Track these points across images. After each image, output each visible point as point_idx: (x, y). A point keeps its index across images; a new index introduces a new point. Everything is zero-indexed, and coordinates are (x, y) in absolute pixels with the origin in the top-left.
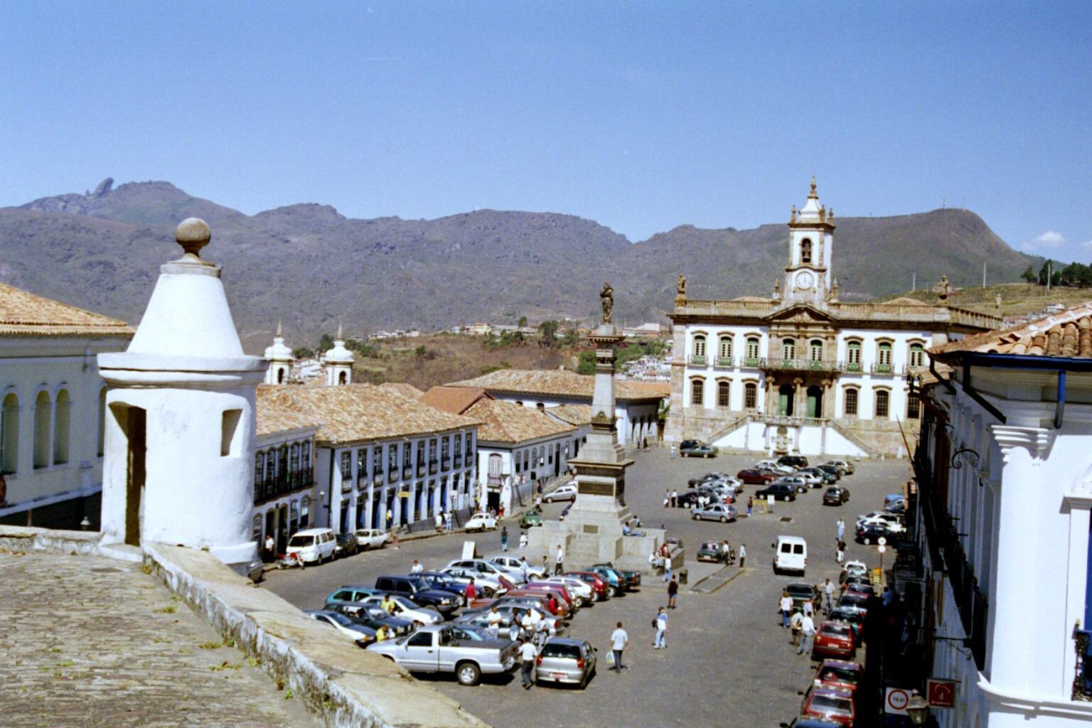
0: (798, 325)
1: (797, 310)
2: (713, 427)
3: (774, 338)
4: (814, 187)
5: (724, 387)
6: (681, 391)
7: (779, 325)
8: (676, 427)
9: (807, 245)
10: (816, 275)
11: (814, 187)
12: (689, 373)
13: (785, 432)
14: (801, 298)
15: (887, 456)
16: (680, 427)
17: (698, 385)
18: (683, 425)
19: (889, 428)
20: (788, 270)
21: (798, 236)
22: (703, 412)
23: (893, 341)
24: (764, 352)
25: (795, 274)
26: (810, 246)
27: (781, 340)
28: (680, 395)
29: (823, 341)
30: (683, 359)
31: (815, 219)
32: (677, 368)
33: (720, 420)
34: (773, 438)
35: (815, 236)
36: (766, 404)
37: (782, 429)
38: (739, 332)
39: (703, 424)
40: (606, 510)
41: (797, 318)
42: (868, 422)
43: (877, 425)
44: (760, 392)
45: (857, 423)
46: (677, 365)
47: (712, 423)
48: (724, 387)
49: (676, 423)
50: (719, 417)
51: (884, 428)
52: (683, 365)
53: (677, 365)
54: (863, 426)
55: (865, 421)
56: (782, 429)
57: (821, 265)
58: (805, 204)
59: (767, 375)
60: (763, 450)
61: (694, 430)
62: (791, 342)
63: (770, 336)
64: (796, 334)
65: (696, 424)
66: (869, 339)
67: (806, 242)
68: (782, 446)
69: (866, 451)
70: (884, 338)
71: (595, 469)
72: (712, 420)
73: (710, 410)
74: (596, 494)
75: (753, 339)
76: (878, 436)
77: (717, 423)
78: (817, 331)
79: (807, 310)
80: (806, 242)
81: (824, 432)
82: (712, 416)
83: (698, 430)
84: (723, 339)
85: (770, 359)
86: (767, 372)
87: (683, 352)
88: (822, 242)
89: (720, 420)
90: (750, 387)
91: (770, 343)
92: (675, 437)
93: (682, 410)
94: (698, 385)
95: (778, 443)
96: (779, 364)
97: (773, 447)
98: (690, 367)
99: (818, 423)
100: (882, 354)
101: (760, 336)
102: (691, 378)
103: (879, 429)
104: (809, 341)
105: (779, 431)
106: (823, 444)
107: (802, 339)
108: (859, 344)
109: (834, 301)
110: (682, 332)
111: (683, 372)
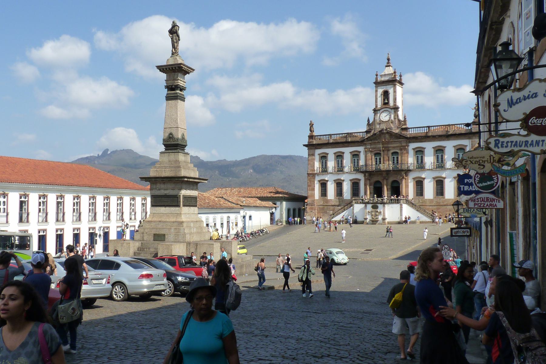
4: (388, 59)
5: (339, 184)
6: (313, 189)
11: (388, 59)
13: (377, 207)
14: (384, 126)
17: (324, 185)
19: (445, 203)
22: (327, 201)
23: (445, 147)
24: (362, 162)
29: (399, 151)
30: (314, 170)
37: (375, 207)
38: (347, 151)
43: (437, 202)
51: (442, 204)
54: (428, 204)
56: (375, 207)
59: (365, 176)
60: (363, 220)
61: (322, 213)
62: (379, 154)
65: (323, 209)
67: (386, 94)
78: (394, 146)
80: (386, 94)
81: (401, 208)
82: (333, 204)
83: (324, 212)
84: (337, 156)
86: (364, 172)
90: (355, 185)
93: (314, 201)
95: (372, 215)
99: (397, 201)
100: (438, 157)
105: (373, 207)
106: (401, 215)
109: (404, 127)
110: (313, 155)
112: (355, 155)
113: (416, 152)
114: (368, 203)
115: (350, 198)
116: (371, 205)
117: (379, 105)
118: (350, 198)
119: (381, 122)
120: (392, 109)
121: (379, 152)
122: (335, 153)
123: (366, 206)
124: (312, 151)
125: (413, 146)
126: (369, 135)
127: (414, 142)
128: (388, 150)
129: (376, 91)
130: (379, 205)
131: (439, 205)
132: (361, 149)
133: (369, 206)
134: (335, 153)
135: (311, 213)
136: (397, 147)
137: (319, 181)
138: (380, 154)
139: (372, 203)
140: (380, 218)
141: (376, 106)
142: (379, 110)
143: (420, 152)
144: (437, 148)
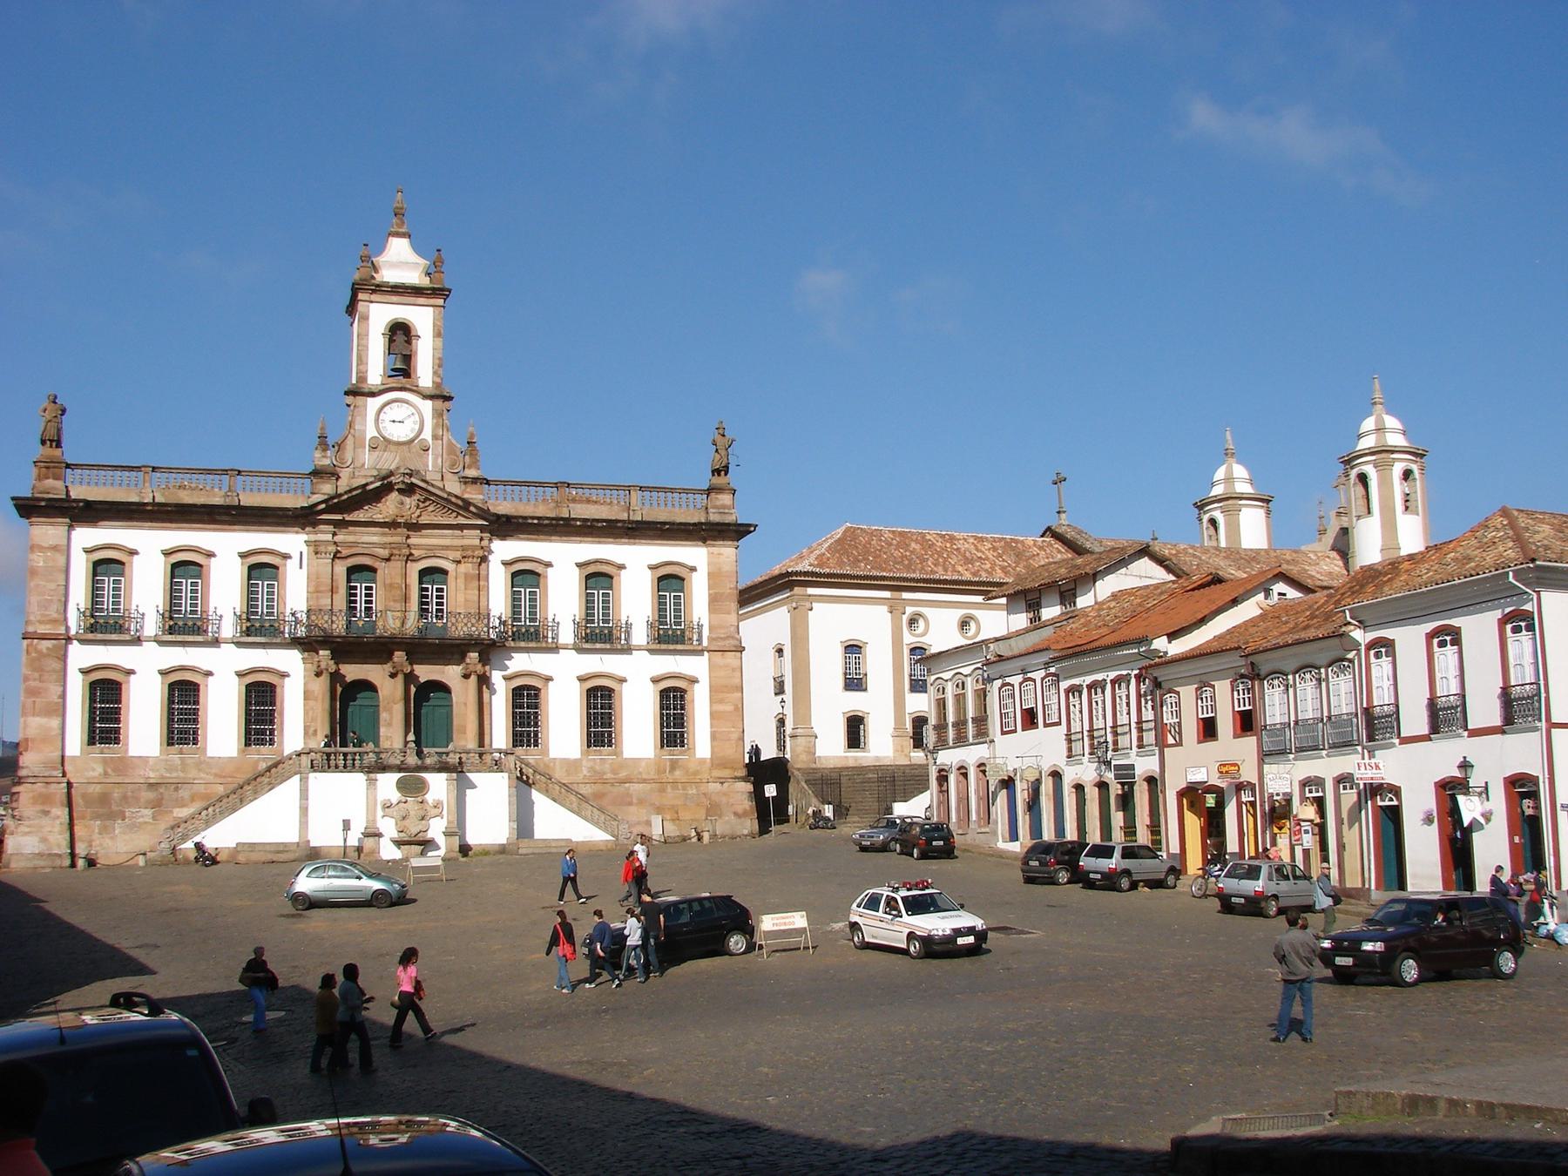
2: (157, 805)
8: (46, 813)
9: (400, 338)
10: (427, 407)
12: (82, 656)
14: (389, 461)
19: (623, 774)
20: (354, 392)
21: (380, 314)
24: (296, 594)
25: (373, 404)
26: (409, 342)
27: (341, 569)
28: (55, 723)
32: (45, 645)
33: (177, 786)
34: (387, 806)
35: (422, 318)
37: (412, 787)
38: (228, 548)
39: (125, 798)
41: (390, 506)
42: (571, 765)
46: (43, 638)
47: (151, 795)
49: (46, 799)
53: (43, 638)
56: (412, 787)
58: (381, 249)
61: (97, 817)
66: (563, 560)
67: (400, 332)
68: (414, 828)
70: (596, 561)
72: (152, 786)
73: (144, 760)
80: (400, 332)
82: (153, 776)
86: (307, 645)
92: (44, 840)
96: (339, 627)
97: (388, 828)
102: (85, 672)
104: (414, 569)
105: (402, 786)
107: (397, 565)
109: (471, 473)
112: (261, 570)
113: (514, 575)
114: (384, 768)
115: (235, 754)
116: (397, 776)
117: (375, 374)
118: (235, 754)
119: (383, 443)
120: (426, 397)
122: (167, 553)
123: (372, 783)
124: (48, 532)
125: (505, 549)
126: (327, 488)
128: (409, 558)
132: (291, 542)
134: (167, 553)
135: (45, 821)
136: (447, 548)
137: (85, 672)
139: (399, 769)
140: (436, 829)
141: (362, 378)
142: (373, 394)
143: (526, 577)
144: (592, 569)
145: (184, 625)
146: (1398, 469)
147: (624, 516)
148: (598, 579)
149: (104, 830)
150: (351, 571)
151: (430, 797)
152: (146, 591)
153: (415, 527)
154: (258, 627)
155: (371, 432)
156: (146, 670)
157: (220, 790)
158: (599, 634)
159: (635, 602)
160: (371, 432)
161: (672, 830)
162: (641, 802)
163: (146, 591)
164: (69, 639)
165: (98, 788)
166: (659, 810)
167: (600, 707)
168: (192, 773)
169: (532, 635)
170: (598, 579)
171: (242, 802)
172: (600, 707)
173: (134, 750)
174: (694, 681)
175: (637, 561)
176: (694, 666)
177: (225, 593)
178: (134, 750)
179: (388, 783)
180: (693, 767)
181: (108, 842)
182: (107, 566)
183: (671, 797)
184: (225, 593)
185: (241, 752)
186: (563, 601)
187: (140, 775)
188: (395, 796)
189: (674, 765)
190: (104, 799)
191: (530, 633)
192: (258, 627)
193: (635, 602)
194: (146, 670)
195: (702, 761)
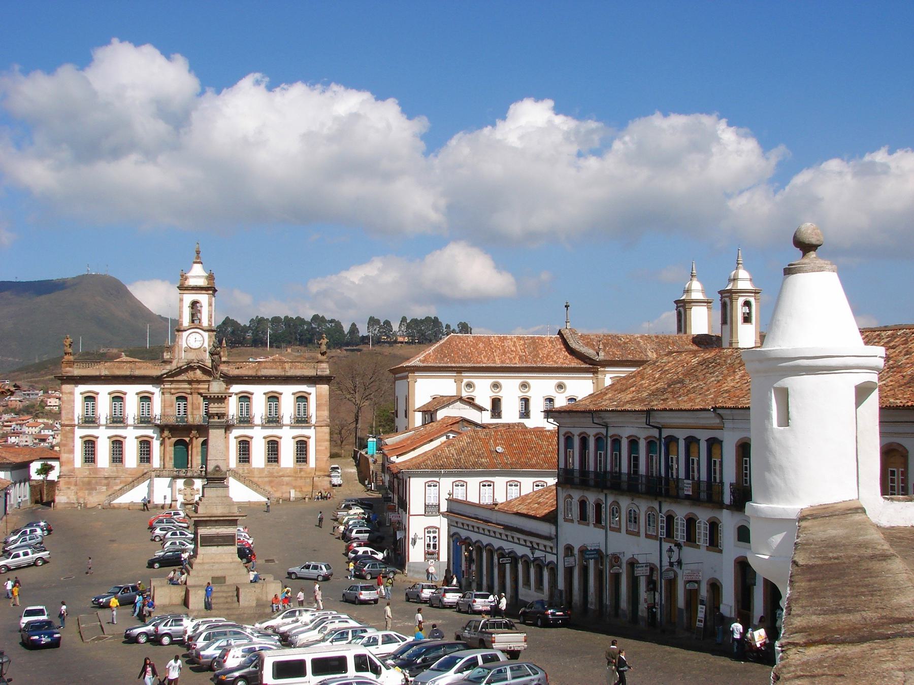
0: (190, 382)
1: (190, 368)
2: (108, 485)
3: (167, 396)
4: (198, 253)
5: (117, 445)
6: (72, 451)
7: (172, 382)
10: (206, 334)
11: (198, 253)
12: (79, 433)
13: (193, 483)
14: (192, 356)
15: (284, 500)
16: (72, 488)
18: (76, 485)
20: (178, 331)
21: (188, 298)
22: (96, 470)
24: (157, 408)
25: (185, 334)
27: (174, 397)
31: (202, 282)
33: (115, 478)
34: (180, 490)
35: (203, 299)
36: (163, 458)
39: (96, 483)
40: (230, 560)
41: (190, 375)
42: (261, 470)
44: (156, 445)
45: (251, 471)
46: (67, 426)
47: (105, 482)
48: (117, 445)
49: (69, 483)
50: (114, 474)
52: (74, 426)
53: (67, 426)
54: (256, 473)
55: (258, 469)
57: (210, 325)
58: (190, 269)
62: (185, 399)
63: (163, 393)
64: (189, 391)
66: (259, 392)
67: (194, 304)
69: (264, 496)
70: (272, 392)
71: (216, 521)
72: (106, 478)
73: (103, 469)
74: (218, 546)
75: (146, 398)
76: (270, 482)
77: (112, 481)
79: (199, 367)
82: (106, 475)
85: (163, 415)
86: (161, 428)
87: (73, 413)
88: (210, 305)
89: (115, 478)
90: (145, 445)
91: (164, 401)
93: (73, 470)
94: (90, 445)
96: (172, 421)
97: (180, 499)
98: (80, 427)
101: (153, 394)
103: (271, 475)
105: (185, 483)
108: (277, 398)
110: (72, 393)
111: (73, 433)
112: (146, 398)
116: (183, 480)
117: (186, 321)
119: (189, 349)
121: (184, 395)
124: (66, 388)
125: (236, 388)
127: (237, 383)
129: (181, 300)
130: (195, 480)
131: (271, 475)
133: (180, 483)
135: (69, 491)
138: (185, 399)
143: (245, 398)
145: (118, 420)
146: (741, 300)
147: (283, 374)
148: (273, 398)
149: (90, 494)
150: (178, 398)
151: (195, 487)
152: (104, 408)
153: (199, 382)
154: (145, 421)
155: (184, 345)
156: (103, 437)
157: (131, 479)
158: (273, 420)
159: (288, 407)
160: (184, 345)
161: (300, 495)
162: (287, 484)
163: (104, 408)
164: (74, 426)
165: (87, 479)
166: (294, 487)
167: (273, 447)
168: (120, 474)
169: (246, 421)
170: (273, 398)
171: (133, 487)
172: (273, 447)
173: (99, 466)
174: (309, 438)
175: (288, 392)
176: (310, 432)
177: (132, 408)
178: (99, 466)
179: (180, 483)
180: (309, 470)
181: (91, 498)
182: (90, 398)
183: (300, 482)
184: (132, 408)
185: (138, 465)
186: (259, 408)
187: (102, 474)
188: (183, 487)
189: (301, 470)
190: (89, 483)
191: (246, 421)
192: (145, 421)
193: (288, 407)
194: (103, 437)
195: (312, 469)
